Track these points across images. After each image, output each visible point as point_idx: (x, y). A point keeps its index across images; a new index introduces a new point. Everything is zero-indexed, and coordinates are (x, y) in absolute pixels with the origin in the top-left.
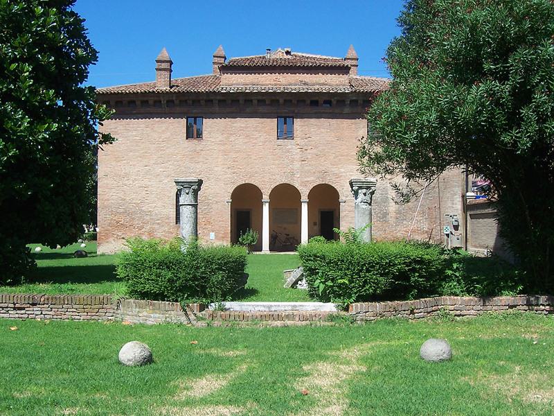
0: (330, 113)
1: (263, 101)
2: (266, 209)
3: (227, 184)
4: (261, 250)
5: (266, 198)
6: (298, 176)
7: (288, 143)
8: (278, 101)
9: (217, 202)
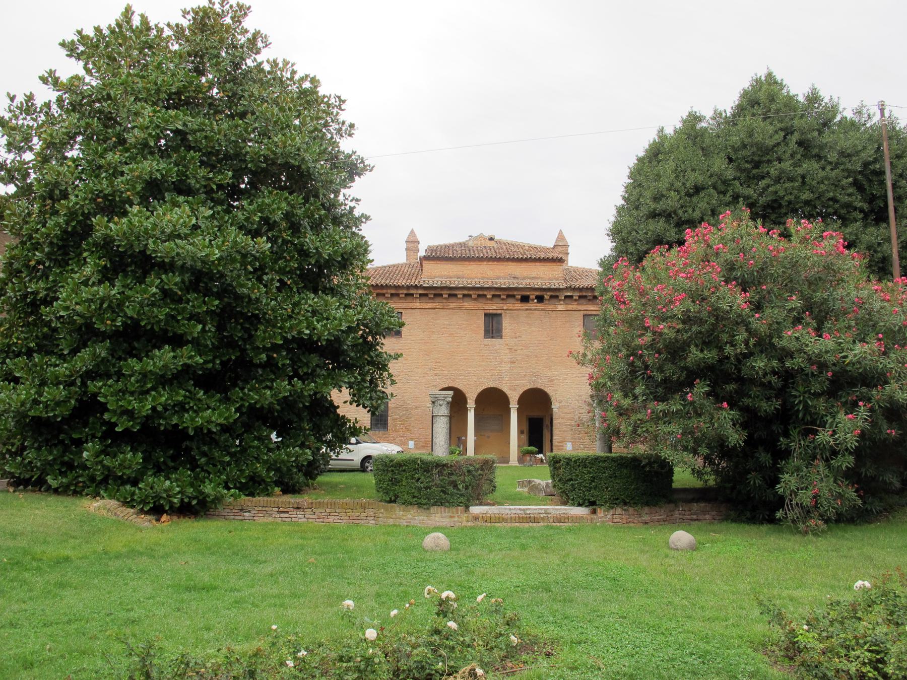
1: (470, 296)
2: (471, 416)
5: (471, 404)
8: (485, 296)
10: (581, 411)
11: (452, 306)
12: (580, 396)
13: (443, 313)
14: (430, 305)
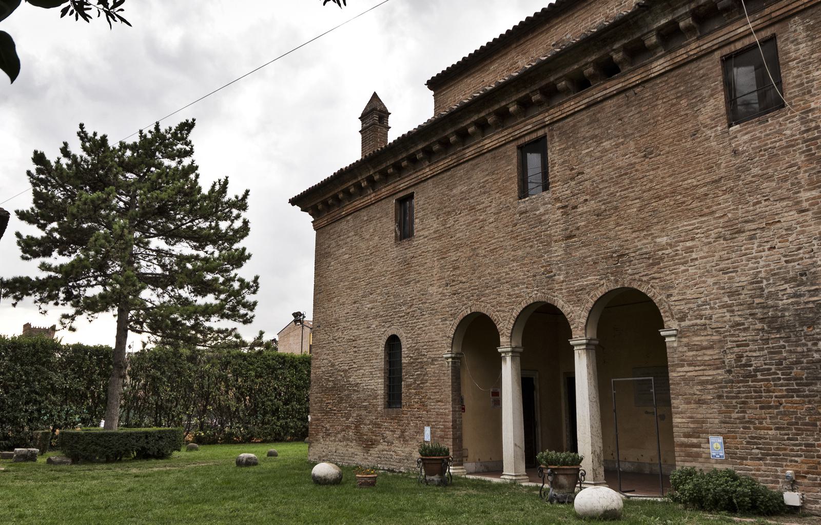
0: (619, 92)
3: (446, 320)
4: (499, 471)
6: (561, 278)
7: (541, 203)
9: (434, 360)
10: (743, 336)
11: (469, 152)
12: (733, 294)
13: (460, 172)
14: (442, 165)
